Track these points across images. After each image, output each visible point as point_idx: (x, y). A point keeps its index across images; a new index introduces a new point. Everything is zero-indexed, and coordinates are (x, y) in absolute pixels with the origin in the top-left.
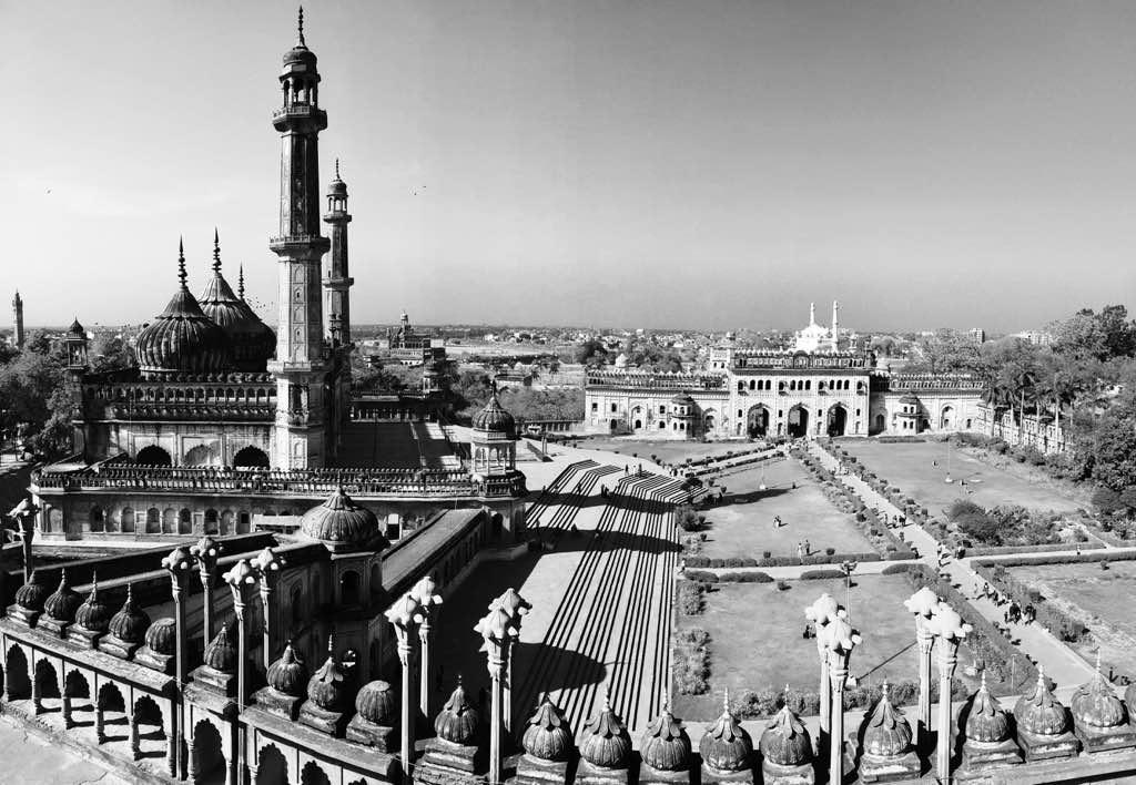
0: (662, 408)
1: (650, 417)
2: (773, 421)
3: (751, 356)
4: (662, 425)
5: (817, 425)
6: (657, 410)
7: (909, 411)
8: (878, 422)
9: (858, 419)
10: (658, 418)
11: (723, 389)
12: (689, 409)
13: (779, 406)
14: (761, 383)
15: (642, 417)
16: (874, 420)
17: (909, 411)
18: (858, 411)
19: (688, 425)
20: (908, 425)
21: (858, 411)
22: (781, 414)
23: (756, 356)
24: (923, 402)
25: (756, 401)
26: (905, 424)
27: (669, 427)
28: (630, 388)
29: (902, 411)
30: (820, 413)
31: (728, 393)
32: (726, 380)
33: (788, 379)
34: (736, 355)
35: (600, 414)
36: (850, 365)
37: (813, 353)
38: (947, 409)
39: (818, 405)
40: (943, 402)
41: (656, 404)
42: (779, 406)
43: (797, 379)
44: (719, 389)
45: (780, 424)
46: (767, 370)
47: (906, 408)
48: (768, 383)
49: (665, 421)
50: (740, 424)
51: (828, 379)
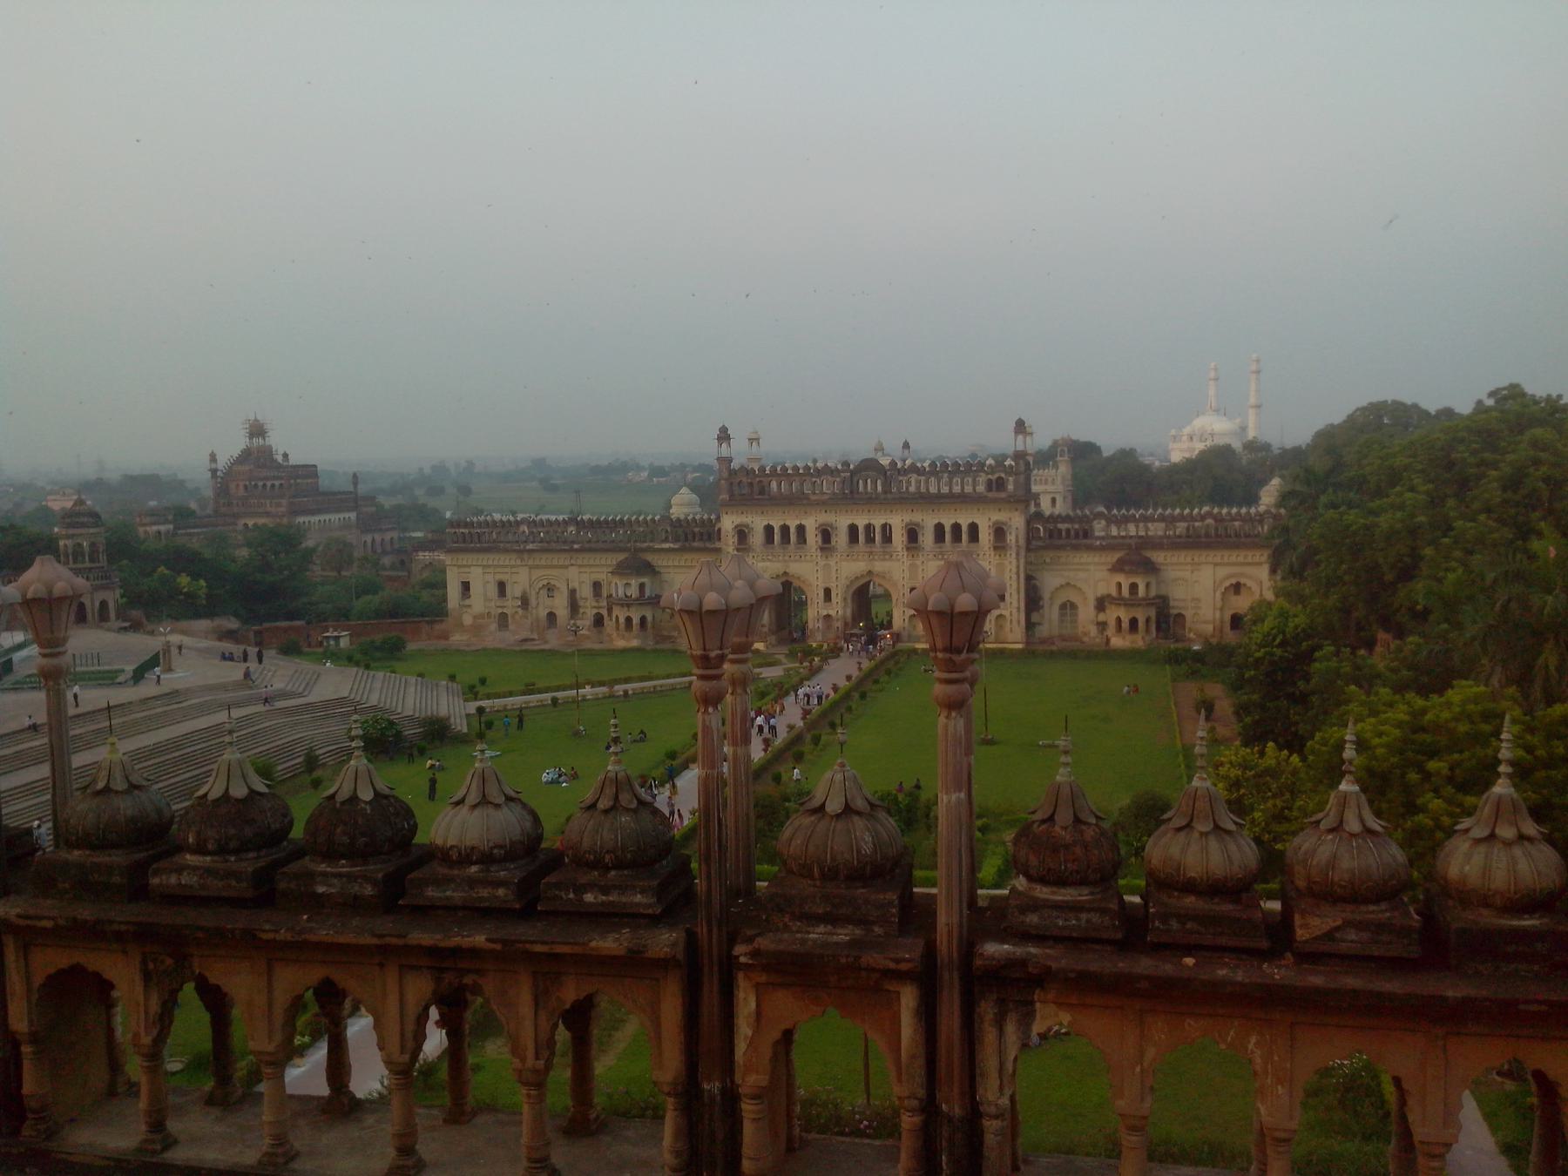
0: (597, 586)
1: (574, 607)
2: (815, 612)
4: (599, 621)
6: (586, 592)
7: (1125, 592)
10: (589, 610)
11: (717, 545)
12: (642, 586)
13: (825, 579)
14: (785, 529)
15: (560, 605)
19: (643, 620)
20: (1126, 625)
22: (828, 592)
24: (1171, 573)
26: (1119, 620)
27: (609, 624)
28: (530, 546)
29: (1114, 593)
33: (842, 521)
35: (477, 603)
37: (893, 463)
40: (1222, 572)
43: (861, 522)
45: (828, 617)
47: (1119, 585)
48: (801, 529)
49: (604, 612)
51: (928, 520)
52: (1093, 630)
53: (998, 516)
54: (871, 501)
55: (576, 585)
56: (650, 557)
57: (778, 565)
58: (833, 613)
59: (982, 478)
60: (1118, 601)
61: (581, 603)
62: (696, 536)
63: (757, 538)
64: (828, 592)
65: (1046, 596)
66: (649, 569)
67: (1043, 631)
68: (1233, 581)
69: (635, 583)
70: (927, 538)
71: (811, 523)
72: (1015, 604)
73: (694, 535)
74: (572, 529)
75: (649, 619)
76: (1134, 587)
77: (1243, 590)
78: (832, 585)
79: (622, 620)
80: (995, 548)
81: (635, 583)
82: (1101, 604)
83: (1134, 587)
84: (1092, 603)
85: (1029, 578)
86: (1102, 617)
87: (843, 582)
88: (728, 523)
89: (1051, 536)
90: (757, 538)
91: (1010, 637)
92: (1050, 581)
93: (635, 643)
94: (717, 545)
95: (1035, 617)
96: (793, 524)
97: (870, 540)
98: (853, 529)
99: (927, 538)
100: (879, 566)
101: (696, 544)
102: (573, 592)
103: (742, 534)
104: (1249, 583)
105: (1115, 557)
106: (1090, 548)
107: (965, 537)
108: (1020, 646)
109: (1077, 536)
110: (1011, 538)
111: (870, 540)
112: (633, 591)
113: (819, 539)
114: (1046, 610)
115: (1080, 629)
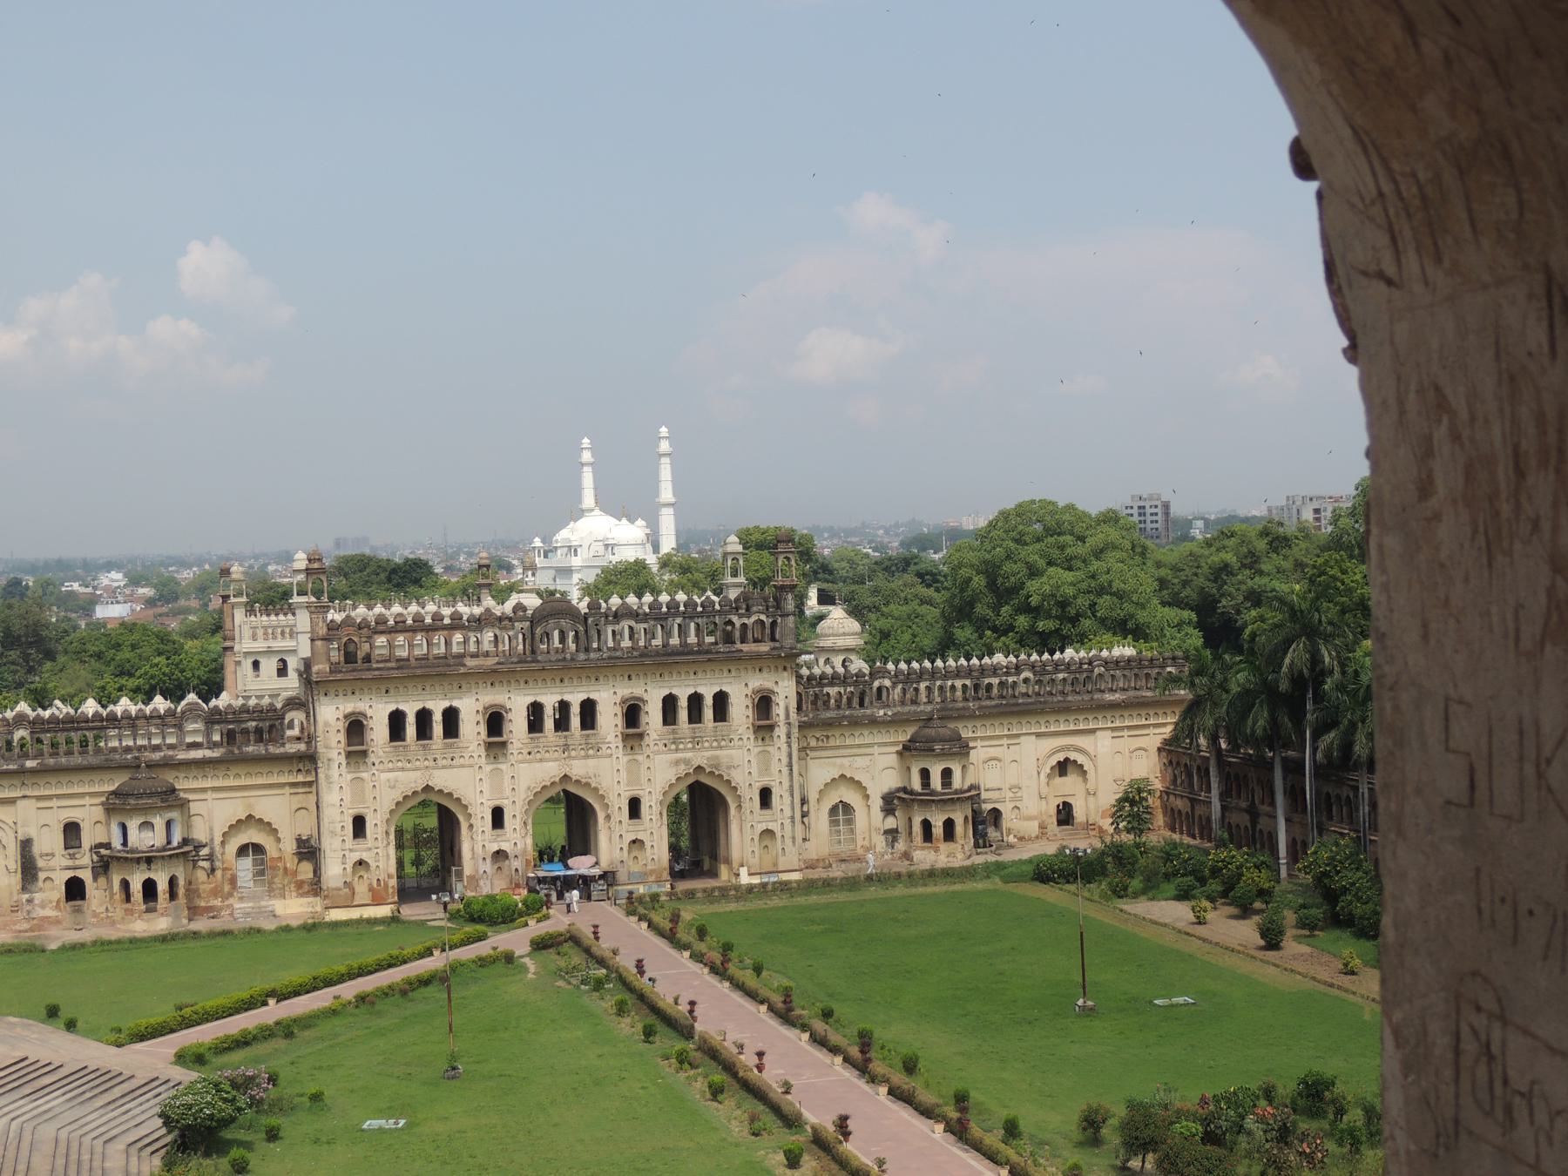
0: (72, 831)
2: (476, 843)
3: (381, 626)
4: (75, 890)
5: (633, 845)
6: (49, 842)
7: (936, 782)
8: (834, 823)
10: (56, 869)
11: (291, 748)
12: (169, 824)
14: (424, 717)
16: (820, 819)
17: (936, 782)
18: (765, 796)
19: (172, 882)
20: (938, 830)
21: (765, 796)
22: (498, 817)
23: (400, 627)
24: (978, 754)
25: (411, 780)
26: (927, 826)
29: (916, 784)
30: (635, 807)
32: (297, 716)
34: (332, 627)
36: (728, 639)
38: (1063, 767)
41: (46, 817)
42: (495, 794)
44: (272, 749)
45: (500, 855)
46: (443, 671)
47: (925, 774)
49: (86, 875)
50: (361, 863)
52: (880, 842)
53: (758, 681)
55: (32, 832)
57: (418, 773)
58: (505, 846)
60: (927, 798)
61: (40, 863)
63: (379, 730)
65: (813, 797)
66: (170, 798)
68: (1061, 757)
69: (159, 822)
71: (471, 708)
72: (788, 812)
73: (246, 732)
74: (20, 734)
75: (181, 882)
76: (947, 774)
77: (1070, 768)
78: (505, 804)
79: (136, 887)
80: (758, 729)
82: (890, 803)
83: (947, 774)
84: (877, 803)
86: (891, 823)
87: (522, 796)
90: (379, 730)
91: (783, 863)
93: (161, 924)
96: (437, 707)
98: (536, 710)
100: (579, 768)
101: (250, 749)
102: (26, 845)
103: (356, 728)
104: (1080, 759)
105: (904, 735)
106: (874, 722)
107: (708, 713)
108: (796, 876)
110: (779, 711)
111: (562, 724)
113: (483, 729)
115: (859, 843)
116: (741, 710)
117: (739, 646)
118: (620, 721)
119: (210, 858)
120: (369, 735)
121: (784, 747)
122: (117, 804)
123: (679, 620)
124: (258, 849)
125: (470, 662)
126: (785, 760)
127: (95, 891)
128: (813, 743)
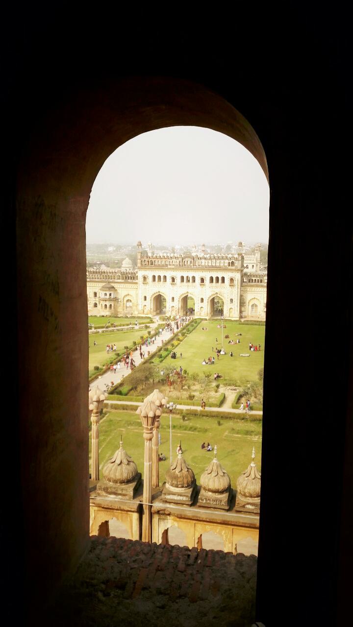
2: (168, 304)
8: (252, 308)
9: (231, 306)
12: (110, 295)
13: (172, 293)
14: (159, 277)
18: (232, 300)
19: (111, 305)
21: (232, 300)
22: (173, 298)
30: (202, 300)
31: (136, 283)
33: (178, 275)
39: (201, 295)
42: (172, 293)
49: (98, 303)
51: (207, 275)
54: (189, 269)
56: (113, 285)
59: (227, 261)
62: (129, 278)
63: (150, 279)
64: (173, 298)
67: (244, 314)
70: (207, 281)
72: (236, 305)
75: (113, 305)
79: (104, 306)
81: (108, 293)
85: (241, 296)
88: (140, 274)
89: (249, 282)
92: (249, 297)
94: (136, 281)
95: (243, 309)
97: (188, 281)
99: (207, 281)
101: (129, 281)
103: (145, 278)
108: (238, 319)
109: (258, 282)
110: (236, 282)
111: (188, 281)
112: (108, 296)
113: (171, 280)
114: (247, 306)
116: (227, 281)
117: (228, 267)
118: (200, 281)
119: (121, 302)
120: (147, 280)
121: (237, 290)
122: (103, 289)
123: (214, 260)
124: (131, 301)
125: (169, 266)
126: (236, 293)
127: (99, 306)
128: (248, 290)
